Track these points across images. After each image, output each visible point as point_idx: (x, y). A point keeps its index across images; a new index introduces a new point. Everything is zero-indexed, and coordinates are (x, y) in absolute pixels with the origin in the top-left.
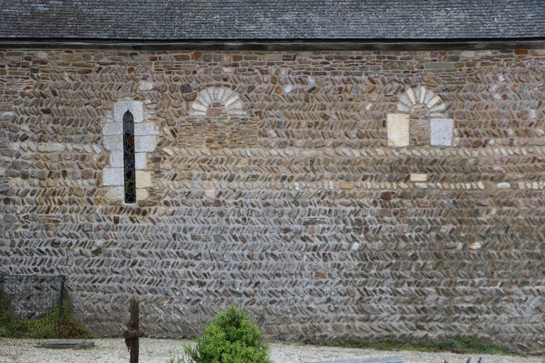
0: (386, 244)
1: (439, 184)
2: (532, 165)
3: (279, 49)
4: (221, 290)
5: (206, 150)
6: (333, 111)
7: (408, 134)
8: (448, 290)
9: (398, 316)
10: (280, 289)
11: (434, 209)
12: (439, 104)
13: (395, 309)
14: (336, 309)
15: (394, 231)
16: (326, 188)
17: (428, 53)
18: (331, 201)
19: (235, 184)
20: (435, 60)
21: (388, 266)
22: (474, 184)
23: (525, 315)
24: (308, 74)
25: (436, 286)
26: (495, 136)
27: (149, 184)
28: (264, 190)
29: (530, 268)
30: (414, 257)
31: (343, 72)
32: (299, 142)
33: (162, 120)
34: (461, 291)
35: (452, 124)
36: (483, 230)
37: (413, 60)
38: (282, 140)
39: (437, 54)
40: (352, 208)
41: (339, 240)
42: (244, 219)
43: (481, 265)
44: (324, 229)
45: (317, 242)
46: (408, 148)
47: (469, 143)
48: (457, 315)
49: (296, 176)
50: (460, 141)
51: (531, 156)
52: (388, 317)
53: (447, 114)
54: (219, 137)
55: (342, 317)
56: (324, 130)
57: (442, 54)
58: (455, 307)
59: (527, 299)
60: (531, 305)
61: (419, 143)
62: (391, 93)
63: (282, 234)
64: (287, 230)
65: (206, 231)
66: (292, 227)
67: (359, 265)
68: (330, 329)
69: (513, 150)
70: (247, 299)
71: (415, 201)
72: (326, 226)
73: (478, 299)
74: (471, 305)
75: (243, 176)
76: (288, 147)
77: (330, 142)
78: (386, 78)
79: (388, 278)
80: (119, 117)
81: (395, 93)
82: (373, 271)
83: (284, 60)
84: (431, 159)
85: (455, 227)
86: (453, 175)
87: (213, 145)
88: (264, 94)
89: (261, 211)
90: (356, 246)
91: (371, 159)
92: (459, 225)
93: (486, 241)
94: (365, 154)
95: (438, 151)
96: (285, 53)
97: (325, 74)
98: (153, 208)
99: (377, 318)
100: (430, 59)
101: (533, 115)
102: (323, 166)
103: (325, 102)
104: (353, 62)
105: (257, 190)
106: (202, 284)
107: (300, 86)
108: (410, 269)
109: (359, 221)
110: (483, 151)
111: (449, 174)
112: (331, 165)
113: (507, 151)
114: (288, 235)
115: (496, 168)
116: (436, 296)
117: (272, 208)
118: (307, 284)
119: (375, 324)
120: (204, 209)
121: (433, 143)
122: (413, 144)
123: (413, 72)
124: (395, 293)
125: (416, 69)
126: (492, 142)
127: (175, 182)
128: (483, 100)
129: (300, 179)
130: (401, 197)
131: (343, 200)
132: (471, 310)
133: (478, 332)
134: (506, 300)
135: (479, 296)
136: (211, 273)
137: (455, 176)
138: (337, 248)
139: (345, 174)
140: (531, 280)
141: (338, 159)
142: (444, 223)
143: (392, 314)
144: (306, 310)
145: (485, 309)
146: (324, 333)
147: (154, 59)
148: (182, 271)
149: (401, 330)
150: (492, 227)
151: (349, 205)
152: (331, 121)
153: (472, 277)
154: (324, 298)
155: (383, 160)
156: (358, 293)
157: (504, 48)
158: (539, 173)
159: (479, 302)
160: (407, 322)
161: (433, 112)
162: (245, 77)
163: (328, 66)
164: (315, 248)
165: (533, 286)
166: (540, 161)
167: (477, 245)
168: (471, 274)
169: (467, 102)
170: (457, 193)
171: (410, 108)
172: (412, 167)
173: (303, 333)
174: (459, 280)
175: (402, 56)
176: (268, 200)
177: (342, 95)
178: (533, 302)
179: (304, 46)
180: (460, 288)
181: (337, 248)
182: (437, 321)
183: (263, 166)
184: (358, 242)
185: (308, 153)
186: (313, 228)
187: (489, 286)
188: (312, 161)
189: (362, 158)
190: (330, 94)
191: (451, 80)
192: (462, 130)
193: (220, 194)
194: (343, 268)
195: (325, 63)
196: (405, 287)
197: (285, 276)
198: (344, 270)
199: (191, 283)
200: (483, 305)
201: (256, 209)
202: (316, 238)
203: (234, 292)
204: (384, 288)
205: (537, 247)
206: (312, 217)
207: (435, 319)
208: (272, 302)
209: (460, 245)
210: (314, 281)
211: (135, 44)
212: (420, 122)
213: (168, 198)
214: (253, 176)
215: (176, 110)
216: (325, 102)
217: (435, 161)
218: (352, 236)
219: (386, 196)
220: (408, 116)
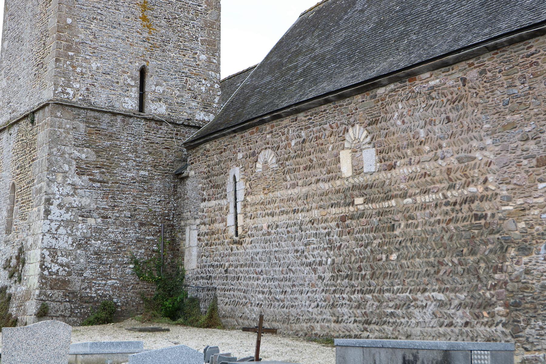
0: (344, 259)
1: (370, 205)
2: (424, 180)
3: (288, 114)
4: (270, 297)
5: (262, 196)
6: (315, 155)
7: (351, 165)
8: (379, 296)
9: (353, 319)
10: (295, 296)
11: (369, 227)
12: (367, 137)
13: (350, 313)
14: (321, 312)
15: (348, 247)
16: (313, 216)
17: (359, 96)
18: (317, 226)
19: (276, 218)
20: (363, 101)
21: (346, 277)
22: (390, 202)
23: (427, 320)
24: (302, 129)
25: (372, 293)
26: (400, 157)
27: (242, 224)
28: (287, 221)
29: (428, 276)
30: (360, 269)
31: (318, 123)
32: (300, 182)
33: (246, 177)
34: (386, 298)
35: (375, 152)
36: (397, 243)
37: (352, 104)
38: (293, 182)
39: (364, 95)
40: (327, 230)
41: (321, 257)
42: (279, 244)
43: (398, 274)
44: (314, 248)
45: (311, 259)
46: (353, 177)
47: (385, 167)
48: (385, 319)
49: (300, 208)
50: (380, 166)
51: (423, 172)
52: (347, 320)
53: (372, 144)
54: (268, 185)
55: (324, 319)
56: (311, 171)
57: (368, 95)
58: (384, 312)
59: (426, 304)
60: (429, 310)
61: (358, 171)
62: (341, 135)
63: (295, 254)
64: (297, 251)
65: (264, 254)
66: (299, 248)
67: (332, 276)
68: (319, 329)
69: (411, 168)
70: (282, 304)
71: (358, 221)
72: (315, 246)
73: (396, 304)
74: (393, 310)
75: (277, 211)
76: (297, 187)
77: (314, 179)
78: (339, 123)
79: (346, 287)
80: (231, 179)
81: (344, 134)
82: (339, 281)
83: (292, 122)
84: (365, 184)
85: (381, 241)
86: (377, 196)
87: (265, 192)
88: (284, 150)
89: (285, 237)
90: (330, 260)
91: (334, 189)
92: (383, 239)
93: (400, 253)
94: (331, 186)
95: (368, 176)
96: (292, 117)
97: (309, 127)
98: (244, 239)
99: (342, 320)
100: (360, 100)
101: (422, 133)
102: (311, 199)
103: (310, 149)
104: (322, 114)
105: (284, 221)
106: (263, 293)
107: (298, 140)
108: (358, 279)
109: (330, 240)
110: (393, 171)
111: (376, 195)
112: (315, 197)
113: (408, 170)
114: (298, 254)
115: (402, 186)
116: (372, 302)
117: (290, 234)
118: (307, 292)
119: (343, 324)
120: (263, 237)
121: (365, 171)
122: (355, 174)
123: (352, 114)
124: (350, 300)
125: (354, 111)
126: (398, 164)
127: (252, 220)
128: (391, 128)
129: (302, 211)
130: (351, 219)
131: (323, 225)
132: (392, 314)
133: (399, 334)
134: (413, 306)
135: (398, 302)
136: (267, 284)
137: (379, 197)
138: (320, 264)
139: (322, 203)
140: (428, 287)
141: (319, 192)
142: (375, 238)
143: (350, 317)
144: (307, 313)
145: (401, 314)
146: (316, 332)
147: (242, 137)
148: (255, 283)
149: (355, 331)
150: (402, 239)
151: (325, 228)
152: (314, 163)
153: (393, 286)
154: (316, 303)
155: (340, 189)
156: (332, 300)
157: (399, 79)
158: (429, 187)
159: (397, 307)
160: (358, 324)
161: (364, 145)
162: (276, 139)
163: (311, 121)
164: (310, 264)
165: (430, 293)
166: (429, 175)
167: (394, 257)
168: (392, 283)
169: (382, 131)
170: (381, 211)
171: (352, 144)
172: (355, 193)
173: (306, 331)
174: (385, 288)
175: (347, 102)
176: (289, 229)
177: (318, 142)
178: (431, 308)
179: (296, 109)
180: (387, 295)
181: (320, 264)
182: (374, 323)
183: (286, 203)
184: (330, 257)
185: (305, 190)
186: (308, 248)
187: (403, 293)
188: (307, 196)
189: (330, 190)
190: (312, 142)
191: (372, 115)
192: (381, 156)
193: (269, 227)
194: (324, 279)
195: (310, 119)
196: (356, 295)
197: (298, 287)
198: (324, 281)
199: (259, 293)
200: (399, 310)
201: (284, 236)
202: (311, 256)
203: (276, 299)
204: (345, 296)
205: (431, 256)
206: (308, 239)
207: (373, 322)
208: (292, 306)
209: (384, 257)
210: (311, 290)
211: (234, 129)
212: (358, 154)
213: (249, 232)
214: (282, 212)
215: (251, 169)
216: (310, 149)
217: (367, 185)
218: (327, 253)
219: (343, 219)
220: (350, 151)
